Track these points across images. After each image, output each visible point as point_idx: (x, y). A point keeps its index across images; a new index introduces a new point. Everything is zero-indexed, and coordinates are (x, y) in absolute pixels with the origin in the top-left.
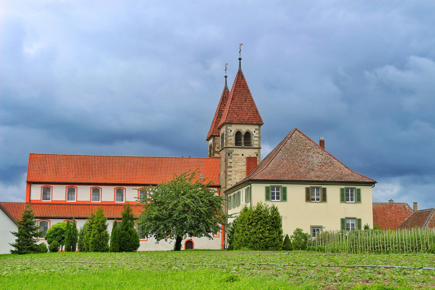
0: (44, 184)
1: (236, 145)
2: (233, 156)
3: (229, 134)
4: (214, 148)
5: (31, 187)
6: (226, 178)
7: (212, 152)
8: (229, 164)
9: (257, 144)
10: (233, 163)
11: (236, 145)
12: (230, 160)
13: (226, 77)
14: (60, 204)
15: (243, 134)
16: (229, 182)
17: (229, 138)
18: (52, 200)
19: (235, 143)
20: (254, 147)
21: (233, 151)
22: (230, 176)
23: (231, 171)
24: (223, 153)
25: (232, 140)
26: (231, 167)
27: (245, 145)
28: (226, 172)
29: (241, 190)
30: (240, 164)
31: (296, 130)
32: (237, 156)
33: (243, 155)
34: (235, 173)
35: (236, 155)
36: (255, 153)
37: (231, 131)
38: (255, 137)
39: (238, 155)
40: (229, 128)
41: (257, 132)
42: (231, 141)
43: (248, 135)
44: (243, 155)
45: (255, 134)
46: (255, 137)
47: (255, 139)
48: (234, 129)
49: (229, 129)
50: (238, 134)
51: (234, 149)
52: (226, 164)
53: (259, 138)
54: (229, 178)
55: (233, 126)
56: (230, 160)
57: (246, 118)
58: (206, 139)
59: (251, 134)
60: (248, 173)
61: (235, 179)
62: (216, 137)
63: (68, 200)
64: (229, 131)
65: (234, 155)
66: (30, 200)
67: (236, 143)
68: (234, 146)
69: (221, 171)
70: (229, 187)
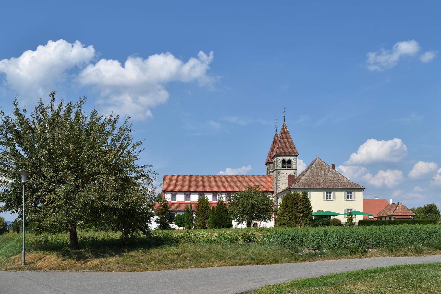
1: (282, 168)
2: (281, 174)
3: (278, 161)
6: (276, 187)
8: (278, 179)
9: (295, 167)
10: (281, 178)
11: (282, 168)
12: (279, 177)
13: (276, 127)
15: (287, 161)
16: (279, 189)
17: (278, 164)
19: (281, 166)
20: (293, 168)
21: (281, 171)
22: (279, 185)
23: (280, 183)
24: (275, 172)
25: (280, 165)
26: (279, 181)
28: (276, 183)
30: (285, 179)
33: (286, 173)
34: (282, 184)
35: (282, 173)
36: (294, 172)
37: (279, 159)
38: (294, 163)
39: (284, 173)
41: (295, 160)
42: (279, 166)
43: (289, 161)
44: (286, 173)
45: (293, 161)
46: (294, 163)
47: (293, 164)
48: (281, 159)
49: (278, 159)
50: (283, 161)
52: (277, 179)
53: (296, 163)
54: (278, 187)
55: (280, 156)
56: (279, 177)
58: (265, 163)
59: (291, 161)
60: (289, 183)
61: (282, 187)
63: (186, 201)
64: (278, 160)
65: (281, 173)
67: (282, 167)
68: (281, 168)
69: (274, 183)
70: (278, 192)
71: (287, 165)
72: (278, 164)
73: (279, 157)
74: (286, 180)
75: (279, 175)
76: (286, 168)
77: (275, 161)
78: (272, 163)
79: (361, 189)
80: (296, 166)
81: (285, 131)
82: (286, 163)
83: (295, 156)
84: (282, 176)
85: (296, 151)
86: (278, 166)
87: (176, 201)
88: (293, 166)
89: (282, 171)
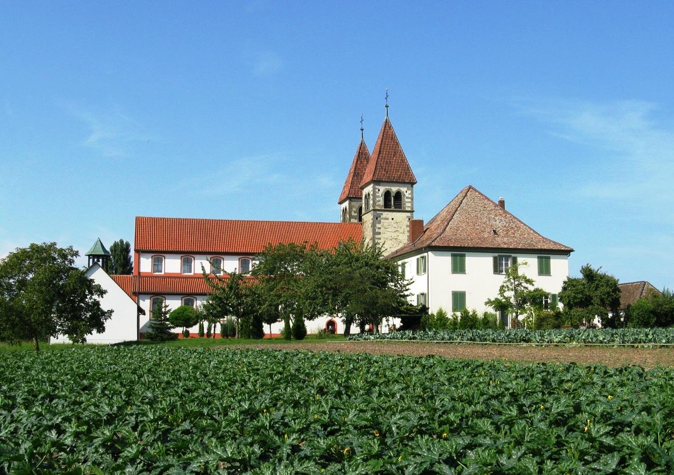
0: (242, 255)
2: (382, 221)
3: (377, 194)
4: (350, 212)
5: (140, 256)
7: (348, 216)
9: (409, 207)
10: (382, 229)
12: (378, 226)
13: (362, 130)
14: (175, 278)
15: (393, 194)
17: (377, 199)
18: (165, 273)
20: (407, 209)
21: (382, 214)
23: (380, 239)
26: (379, 233)
27: (395, 208)
29: (406, 260)
31: (470, 187)
32: (387, 221)
33: (393, 219)
36: (407, 217)
38: (407, 198)
39: (388, 219)
40: (377, 187)
41: (409, 192)
42: (380, 203)
43: (398, 195)
44: (393, 219)
45: (407, 195)
46: (407, 198)
47: (407, 200)
49: (377, 188)
50: (387, 194)
53: (412, 199)
56: (378, 226)
57: (396, 175)
62: (352, 200)
64: (377, 190)
65: (382, 219)
66: (139, 273)
68: (383, 208)
71: (394, 202)
72: (377, 199)
73: (380, 185)
74: (392, 232)
75: (380, 223)
76: (393, 208)
77: (369, 194)
78: (360, 200)
79: (566, 252)
80: (412, 205)
81: (388, 137)
82: (392, 198)
83: (410, 185)
84: (385, 225)
85: (412, 175)
87: (161, 272)
88: (407, 205)
89: (385, 214)
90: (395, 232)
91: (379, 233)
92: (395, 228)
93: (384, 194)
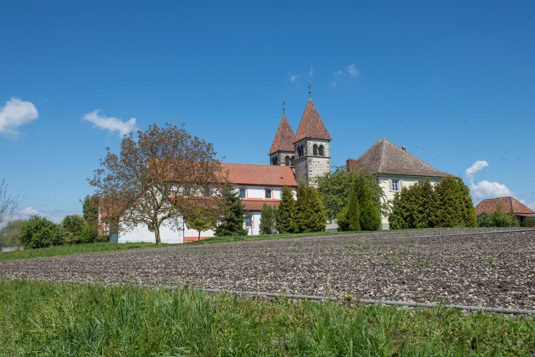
2: (312, 163)
9: (328, 155)
12: (310, 166)
15: (318, 147)
17: (309, 149)
20: (326, 156)
21: (312, 159)
23: (311, 175)
25: (310, 151)
26: (311, 171)
32: (315, 163)
33: (318, 162)
36: (327, 161)
37: (310, 144)
38: (326, 149)
39: (316, 162)
44: (318, 162)
45: (326, 147)
46: (326, 149)
47: (326, 151)
50: (315, 146)
51: (313, 158)
55: (311, 140)
64: (309, 144)
68: (313, 155)
73: (310, 140)
86: (309, 152)
89: (314, 159)
90: (320, 170)
91: (311, 171)
92: (320, 168)
93: (313, 146)
